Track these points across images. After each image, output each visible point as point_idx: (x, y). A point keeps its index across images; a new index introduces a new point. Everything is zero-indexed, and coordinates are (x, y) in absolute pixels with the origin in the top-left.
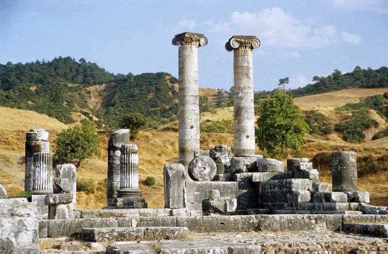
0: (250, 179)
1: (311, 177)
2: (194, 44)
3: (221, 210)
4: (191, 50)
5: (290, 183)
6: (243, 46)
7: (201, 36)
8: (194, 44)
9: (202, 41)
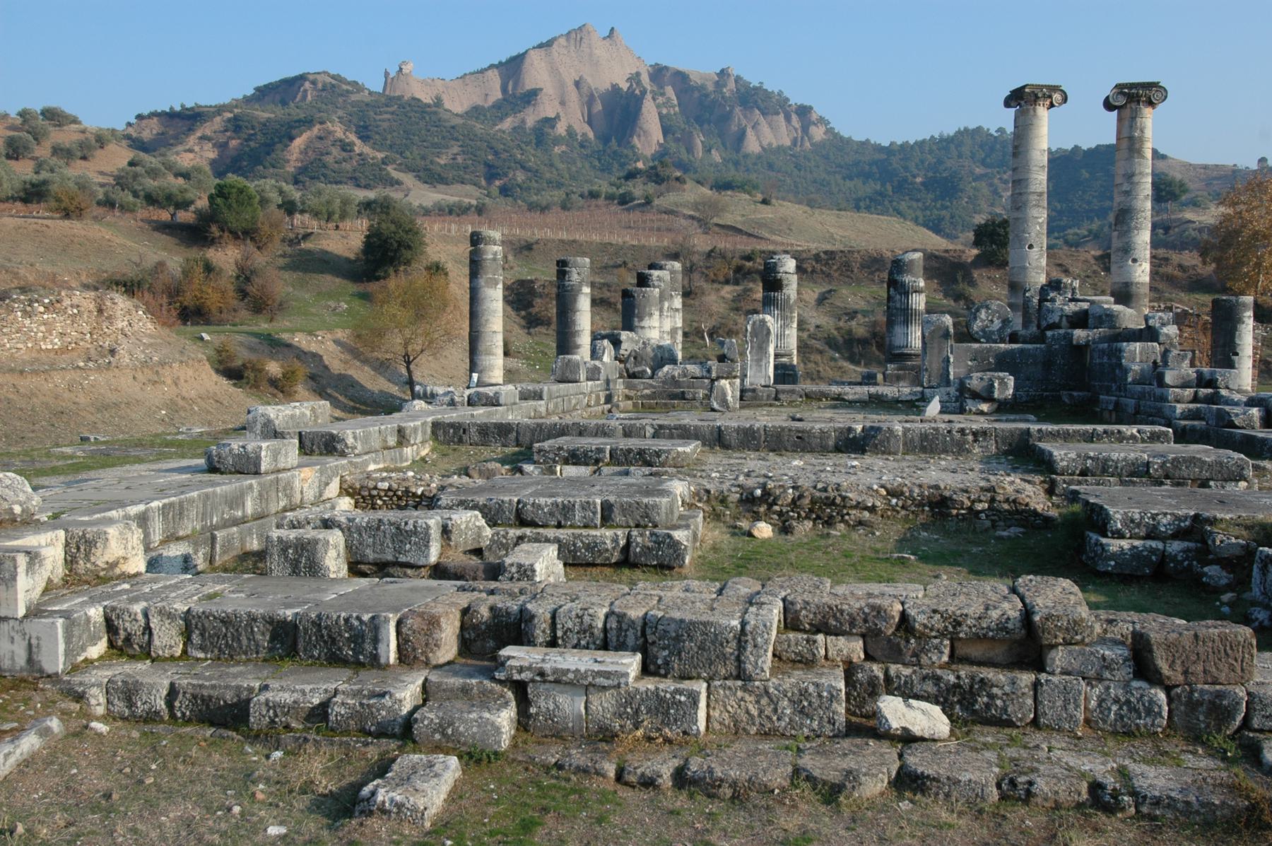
0: (1069, 337)
1: (1162, 339)
3: (984, 395)
5: (1120, 351)
7: (1056, 89)
9: (1057, 97)
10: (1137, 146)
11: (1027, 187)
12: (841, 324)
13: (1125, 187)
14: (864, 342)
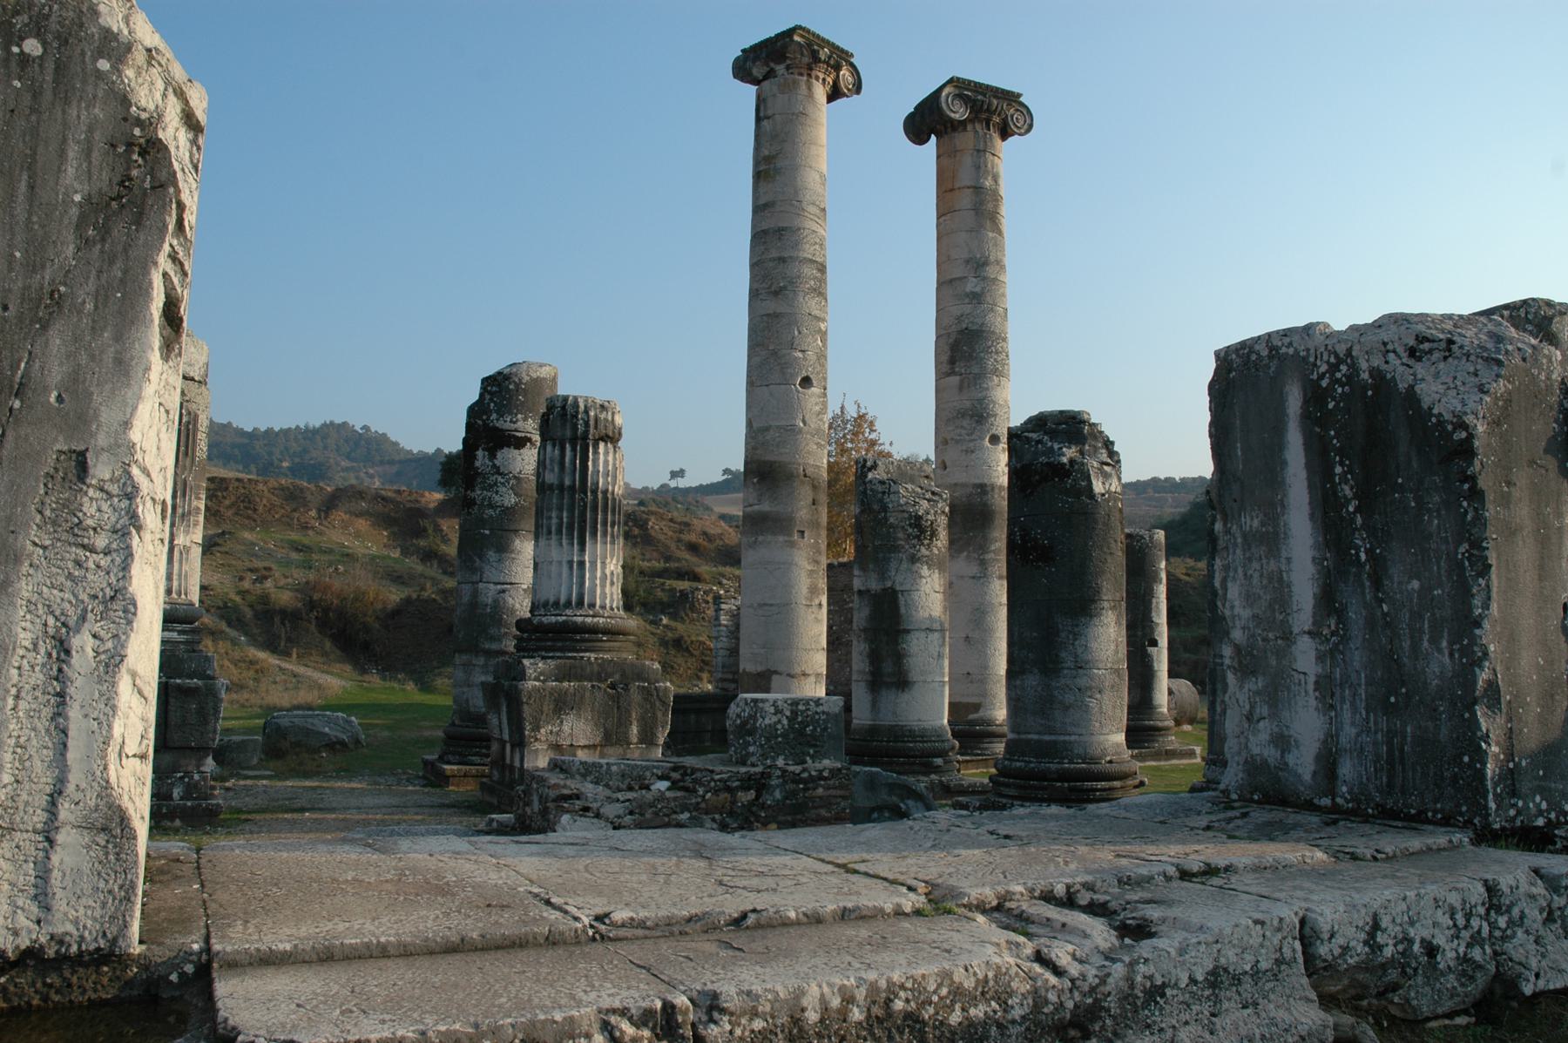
2: (821, 76)
4: (810, 95)
6: (980, 121)
7: (840, 58)
8: (821, 76)
10: (990, 206)
11: (796, 245)
12: (246, 585)
13: (971, 286)
14: (290, 616)
